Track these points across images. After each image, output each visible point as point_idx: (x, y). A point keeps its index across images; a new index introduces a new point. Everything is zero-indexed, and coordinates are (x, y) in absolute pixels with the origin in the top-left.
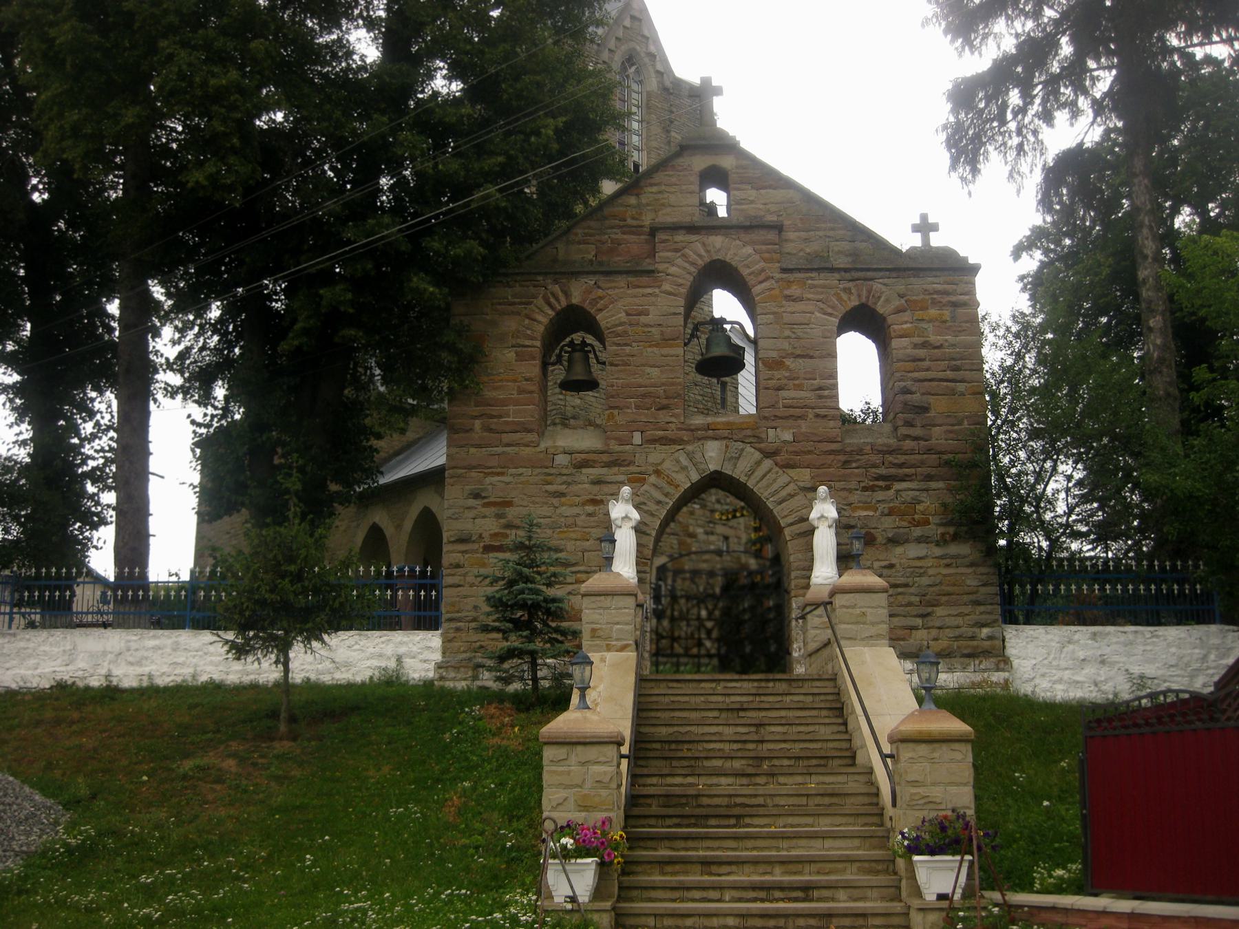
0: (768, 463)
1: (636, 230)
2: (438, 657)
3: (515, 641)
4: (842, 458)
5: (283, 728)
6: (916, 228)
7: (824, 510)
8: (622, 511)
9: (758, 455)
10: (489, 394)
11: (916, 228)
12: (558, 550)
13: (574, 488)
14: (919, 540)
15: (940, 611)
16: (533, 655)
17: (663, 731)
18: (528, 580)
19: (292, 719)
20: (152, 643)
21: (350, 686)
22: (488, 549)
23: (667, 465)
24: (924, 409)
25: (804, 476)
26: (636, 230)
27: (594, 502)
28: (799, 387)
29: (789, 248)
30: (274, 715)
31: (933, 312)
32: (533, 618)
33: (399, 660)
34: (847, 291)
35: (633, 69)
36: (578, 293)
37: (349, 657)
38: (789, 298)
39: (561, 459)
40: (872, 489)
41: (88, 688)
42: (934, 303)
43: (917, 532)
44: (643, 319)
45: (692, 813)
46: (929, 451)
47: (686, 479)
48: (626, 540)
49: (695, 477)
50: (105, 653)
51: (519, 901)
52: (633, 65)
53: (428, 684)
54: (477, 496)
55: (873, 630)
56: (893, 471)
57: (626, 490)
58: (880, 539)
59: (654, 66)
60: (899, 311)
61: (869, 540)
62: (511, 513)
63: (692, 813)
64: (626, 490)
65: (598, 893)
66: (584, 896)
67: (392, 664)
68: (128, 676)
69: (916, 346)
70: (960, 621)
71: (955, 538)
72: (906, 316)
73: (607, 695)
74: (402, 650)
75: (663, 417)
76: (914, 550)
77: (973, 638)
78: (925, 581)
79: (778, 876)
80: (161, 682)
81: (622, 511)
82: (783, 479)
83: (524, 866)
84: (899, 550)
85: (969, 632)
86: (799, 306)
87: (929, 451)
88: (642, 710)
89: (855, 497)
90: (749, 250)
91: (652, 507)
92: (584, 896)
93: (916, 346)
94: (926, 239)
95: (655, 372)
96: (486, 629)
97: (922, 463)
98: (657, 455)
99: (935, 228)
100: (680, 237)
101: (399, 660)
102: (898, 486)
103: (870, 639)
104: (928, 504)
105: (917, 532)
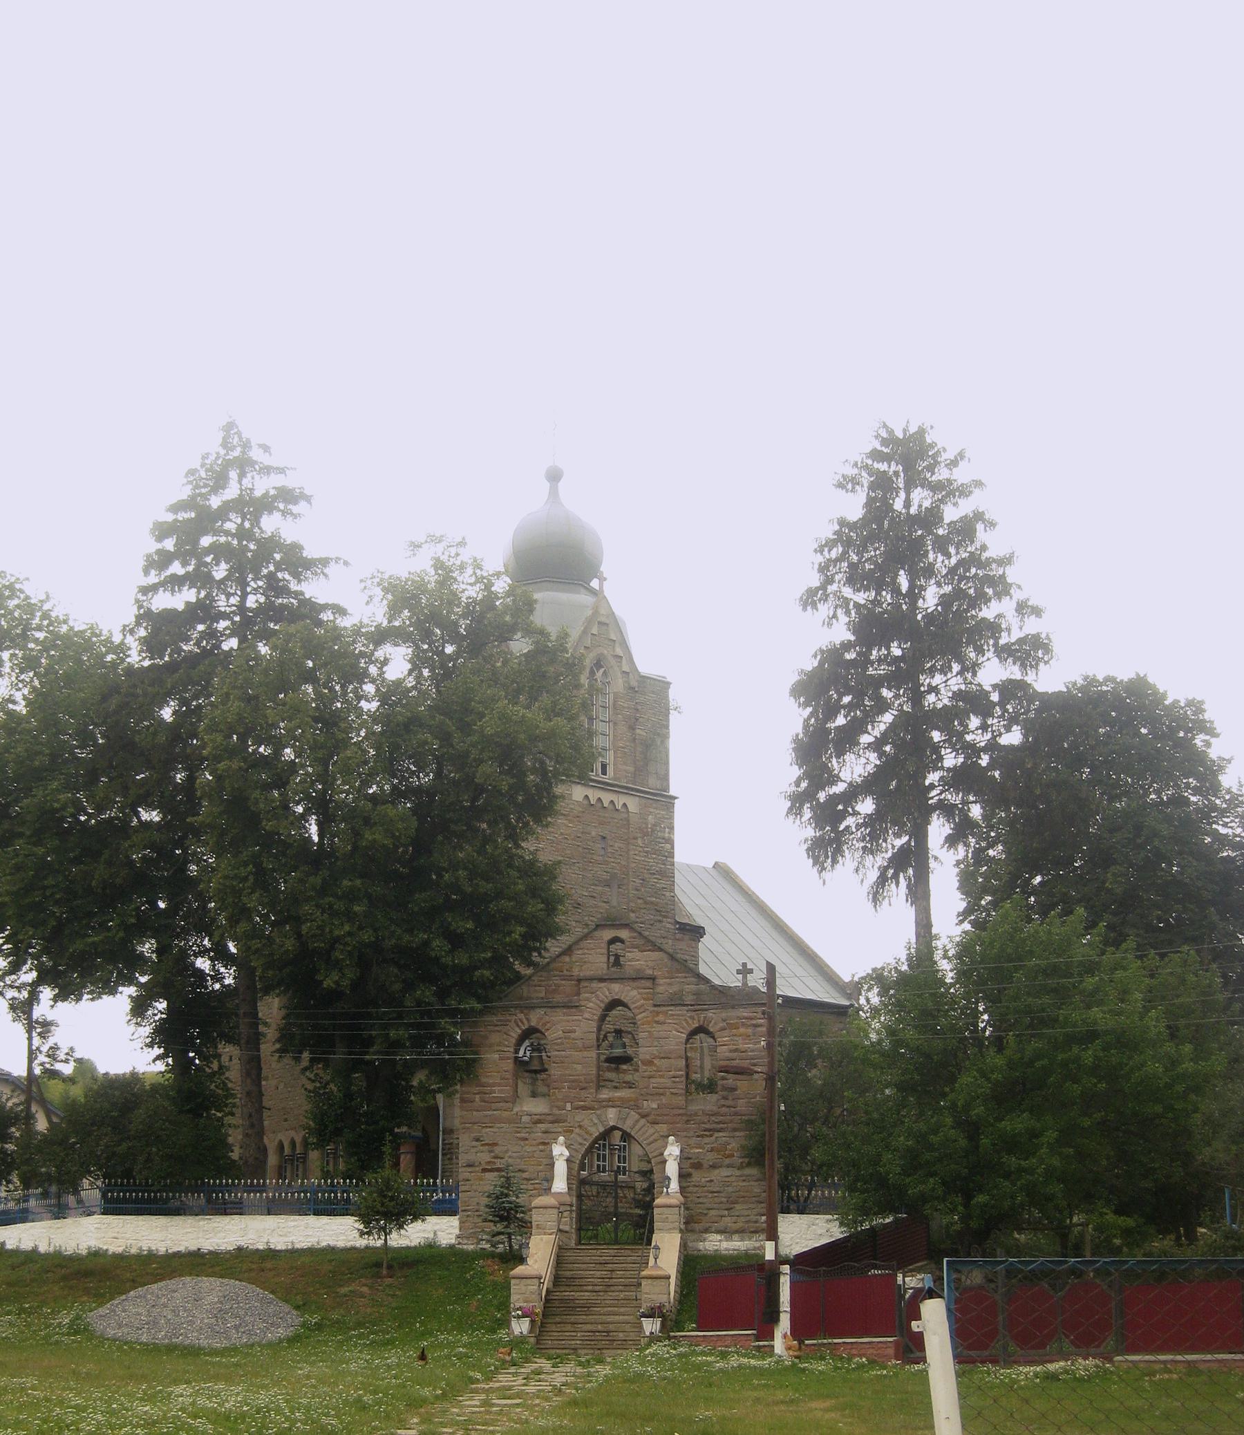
0: (643, 1121)
1: (570, 978)
2: (457, 1231)
3: (500, 1227)
4: (685, 1118)
5: (385, 1272)
6: (739, 972)
7: (673, 1150)
8: (560, 1151)
9: (637, 1116)
10: (484, 1080)
11: (739, 972)
12: (523, 1171)
13: (533, 1135)
14: (728, 1166)
15: (738, 1207)
16: (509, 1235)
17: (568, 1274)
18: (507, 1195)
19: (390, 1267)
20: (293, 1224)
21: (408, 1248)
22: (484, 1170)
23: (586, 1123)
24: (734, 1089)
25: (663, 1128)
26: (570, 978)
27: (544, 1144)
28: (661, 1076)
29: (660, 989)
30: (378, 1265)
31: (742, 1030)
32: (508, 1216)
33: (435, 1233)
34: (692, 1018)
35: (602, 670)
36: (535, 1019)
37: (414, 1234)
38: (657, 1022)
39: (525, 1119)
40: (702, 1136)
41: (257, 1250)
42: (743, 1025)
43: (727, 1161)
44: (572, 1035)
45: (571, 1307)
46: (736, 1114)
47: (596, 1131)
48: (561, 1169)
49: (602, 1129)
50: (264, 1230)
51: (502, 1334)
52: (601, 667)
53: (452, 1247)
54: (478, 1140)
55: (672, 1226)
56: (715, 1126)
57: (561, 1139)
58: (706, 1166)
59: (620, 667)
60: (723, 1029)
61: (698, 1166)
62: (497, 1150)
63: (571, 1307)
64: (561, 1139)
65: (531, 1331)
66: (525, 1332)
67: (431, 1236)
68: (279, 1244)
69: (731, 1051)
70: (749, 1212)
71: (749, 1165)
72: (726, 1033)
73: (540, 1254)
74: (436, 1228)
75: (583, 1094)
76: (725, 1172)
77: (756, 1222)
78: (730, 1189)
79: (600, 1327)
80: (298, 1246)
81: (560, 1151)
82: (651, 1131)
83: (505, 1323)
84: (717, 1171)
85: (754, 1218)
86: (665, 1027)
87: (736, 1114)
88: (559, 1262)
89: (693, 1141)
90: (634, 993)
91: (576, 1146)
92: (525, 1332)
93: (731, 1051)
94: (745, 978)
95: (579, 1067)
96: (485, 1220)
97: (731, 1121)
98: (580, 1116)
99: (751, 971)
100: (595, 985)
101: (435, 1233)
102: (716, 1134)
103: (669, 1230)
104: (734, 1145)
105: (727, 1161)
